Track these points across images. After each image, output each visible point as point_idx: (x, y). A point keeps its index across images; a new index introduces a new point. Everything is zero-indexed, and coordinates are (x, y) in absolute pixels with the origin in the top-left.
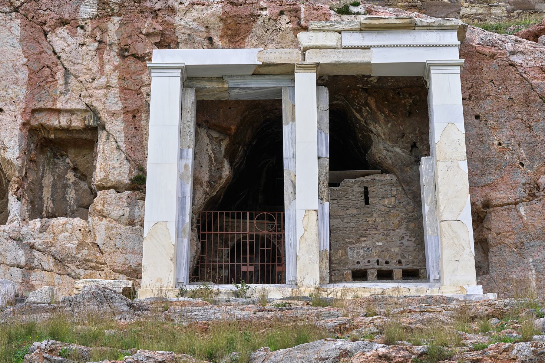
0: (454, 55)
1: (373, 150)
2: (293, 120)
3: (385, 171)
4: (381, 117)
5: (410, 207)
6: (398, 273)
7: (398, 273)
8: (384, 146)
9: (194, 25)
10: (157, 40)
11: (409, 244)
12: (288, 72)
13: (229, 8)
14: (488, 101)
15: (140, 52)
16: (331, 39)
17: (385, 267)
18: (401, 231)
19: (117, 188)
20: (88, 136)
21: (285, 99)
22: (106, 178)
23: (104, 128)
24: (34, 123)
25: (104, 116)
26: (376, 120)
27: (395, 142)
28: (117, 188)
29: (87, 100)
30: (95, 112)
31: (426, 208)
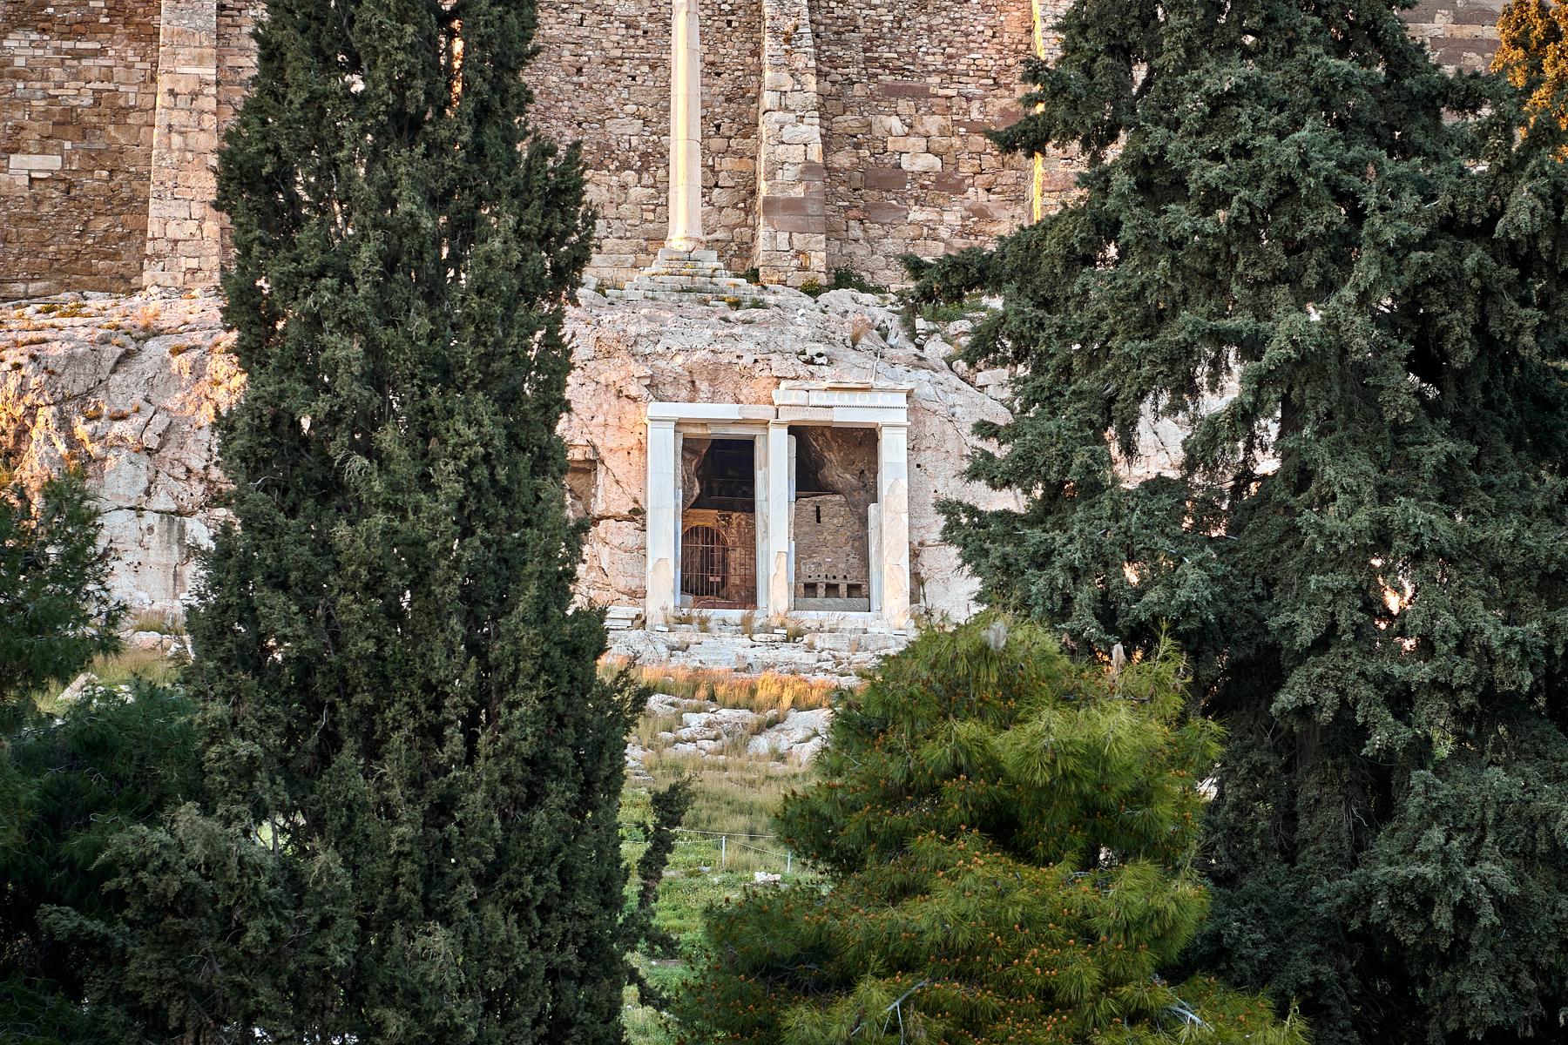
0: (901, 417)
1: (825, 471)
2: (767, 465)
3: (836, 492)
4: (835, 446)
5: (856, 527)
6: (843, 589)
7: (843, 589)
8: (836, 471)
9: (679, 370)
10: (647, 382)
11: (855, 561)
13: (710, 356)
14: (929, 452)
15: (633, 394)
16: (798, 397)
17: (833, 582)
18: (848, 548)
19: (618, 518)
20: (587, 466)
21: (758, 445)
22: (607, 509)
23: (603, 462)
25: (603, 453)
26: (831, 450)
27: (846, 470)
28: (618, 518)
29: (588, 437)
30: (594, 447)
31: (873, 549)
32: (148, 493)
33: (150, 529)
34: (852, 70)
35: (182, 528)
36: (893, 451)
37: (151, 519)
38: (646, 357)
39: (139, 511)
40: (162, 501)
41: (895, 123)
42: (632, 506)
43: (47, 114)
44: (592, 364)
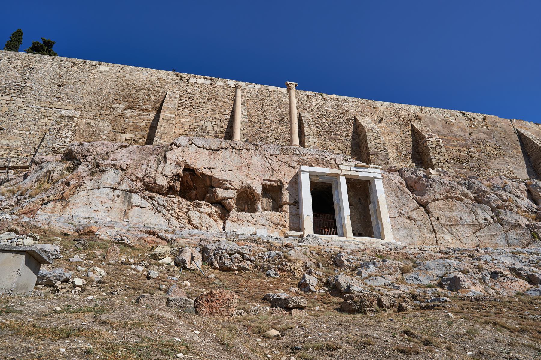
9: (308, 160)
12: (337, 176)
15: (293, 166)
18: (357, 222)
24: (263, 183)
32: (119, 184)
33: (118, 196)
34: (321, 133)
35: (130, 198)
36: (379, 185)
37: (117, 192)
38: (296, 155)
39: (114, 189)
40: (124, 187)
41: (331, 143)
42: (294, 201)
43: (132, 126)
44: (279, 156)
